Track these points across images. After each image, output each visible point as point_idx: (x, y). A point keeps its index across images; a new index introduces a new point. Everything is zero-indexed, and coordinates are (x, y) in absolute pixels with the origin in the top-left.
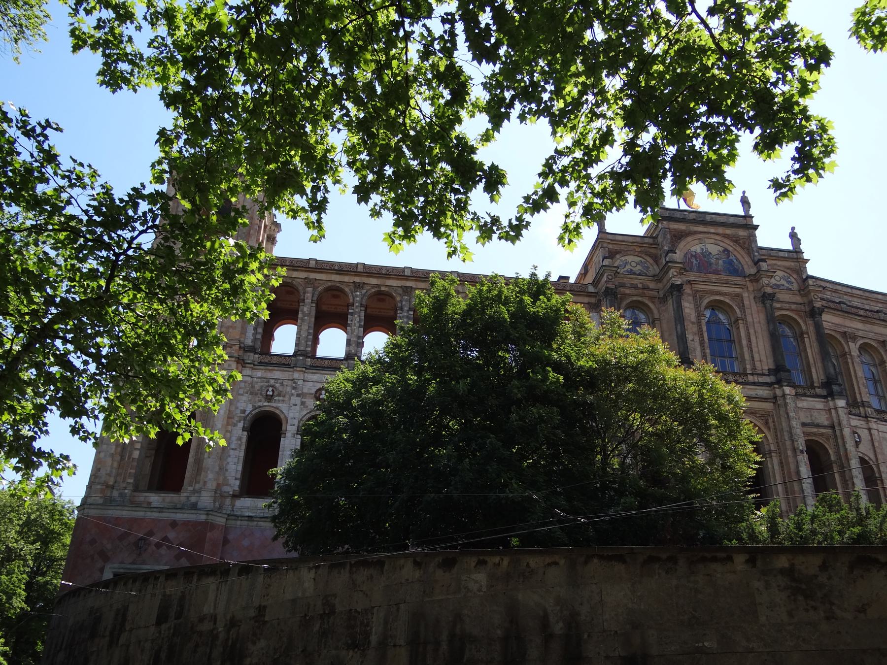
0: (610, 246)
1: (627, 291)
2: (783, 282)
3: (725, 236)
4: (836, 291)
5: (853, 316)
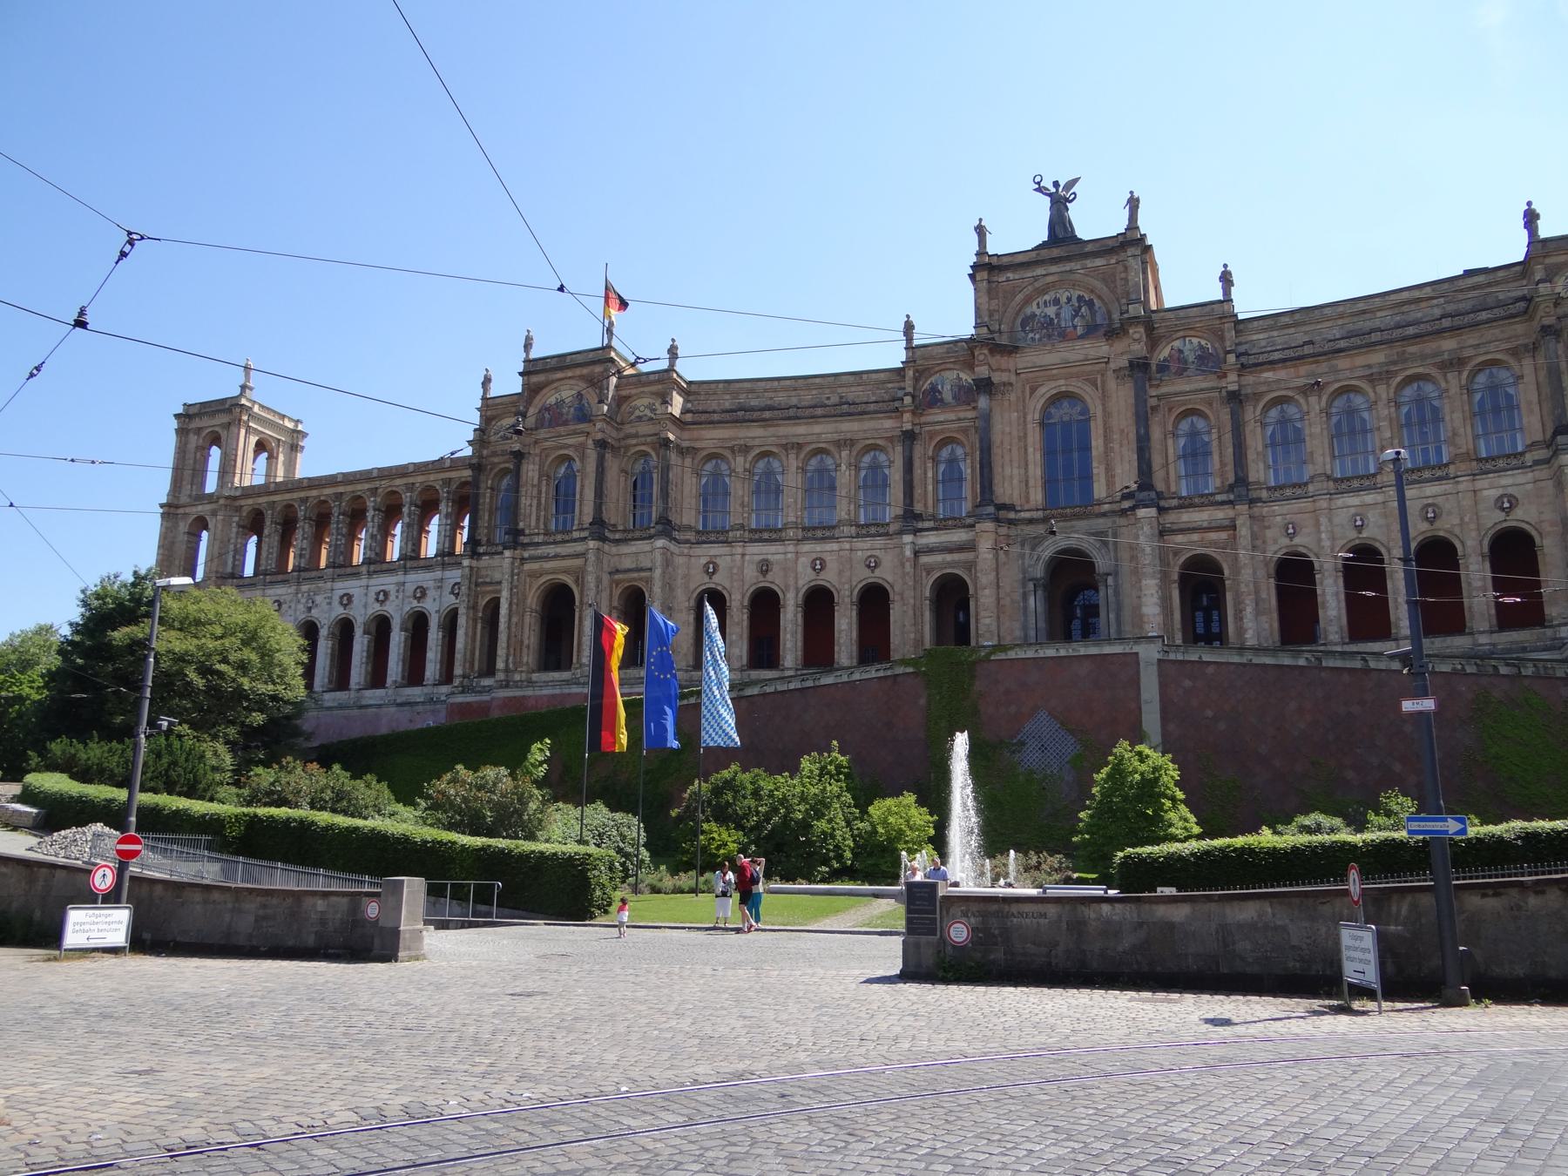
0: (489, 413)
1: (496, 460)
2: (648, 412)
3: (582, 377)
4: (752, 391)
5: (748, 424)
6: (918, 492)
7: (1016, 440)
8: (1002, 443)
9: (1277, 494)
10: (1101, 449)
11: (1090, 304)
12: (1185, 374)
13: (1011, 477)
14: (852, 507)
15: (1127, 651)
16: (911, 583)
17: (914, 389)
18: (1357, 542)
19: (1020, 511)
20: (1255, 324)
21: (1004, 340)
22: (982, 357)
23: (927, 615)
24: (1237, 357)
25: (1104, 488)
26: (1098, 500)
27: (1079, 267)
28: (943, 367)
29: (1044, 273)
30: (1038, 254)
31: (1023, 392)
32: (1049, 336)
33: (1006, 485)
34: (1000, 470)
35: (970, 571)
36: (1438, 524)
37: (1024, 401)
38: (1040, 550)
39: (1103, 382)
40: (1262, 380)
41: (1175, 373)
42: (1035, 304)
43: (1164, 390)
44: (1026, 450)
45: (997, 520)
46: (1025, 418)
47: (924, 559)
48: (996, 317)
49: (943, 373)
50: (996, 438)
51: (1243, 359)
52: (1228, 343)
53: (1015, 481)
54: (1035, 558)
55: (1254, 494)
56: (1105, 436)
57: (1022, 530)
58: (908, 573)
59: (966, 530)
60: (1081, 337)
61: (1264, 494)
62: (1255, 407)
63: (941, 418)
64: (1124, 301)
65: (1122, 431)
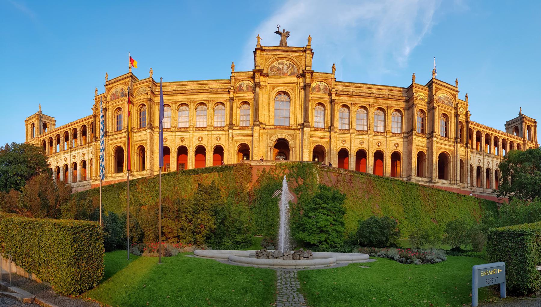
6: (234, 117)
9: (341, 132)
14: (212, 121)
18: (361, 148)
36: (380, 147)
61: (338, 131)
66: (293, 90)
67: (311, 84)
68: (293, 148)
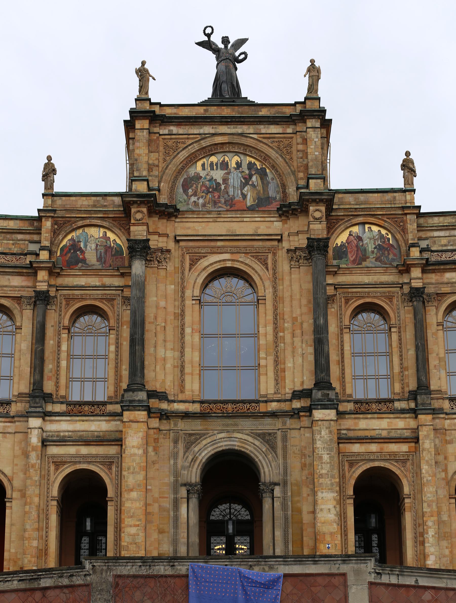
6: (49, 367)
7: (171, 317)
8: (156, 318)
10: (270, 337)
11: (262, 174)
12: (364, 264)
13: (164, 359)
15: (334, 571)
16: (37, 478)
17: (52, 243)
19: (174, 401)
20: (436, 220)
21: (163, 199)
22: (139, 216)
23: (54, 519)
24: (421, 252)
25: (272, 383)
26: (266, 396)
27: (251, 131)
28: (87, 222)
29: (212, 131)
30: (206, 111)
31: (182, 262)
32: (215, 203)
33: (158, 368)
34: (152, 350)
35: (110, 469)
37: (183, 273)
38: (196, 449)
39: (275, 262)
40: (445, 280)
41: (354, 262)
42: (199, 164)
43: (341, 279)
44: (183, 329)
45: (148, 410)
46: (183, 292)
47: (53, 450)
48: (155, 172)
49: (86, 230)
50: (150, 312)
51: (426, 255)
52: (410, 236)
53: (168, 366)
54: (190, 458)
55: (436, 404)
56: (275, 324)
57: (176, 425)
58: (33, 466)
59: (107, 418)
60: (251, 209)
61: (446, 405)
62: (437, 308)
63: (82, 281)
64: (301, 175)
65: (294, 319)
66: (266, 265)
67: (328, 239)
68: (277, 491)
